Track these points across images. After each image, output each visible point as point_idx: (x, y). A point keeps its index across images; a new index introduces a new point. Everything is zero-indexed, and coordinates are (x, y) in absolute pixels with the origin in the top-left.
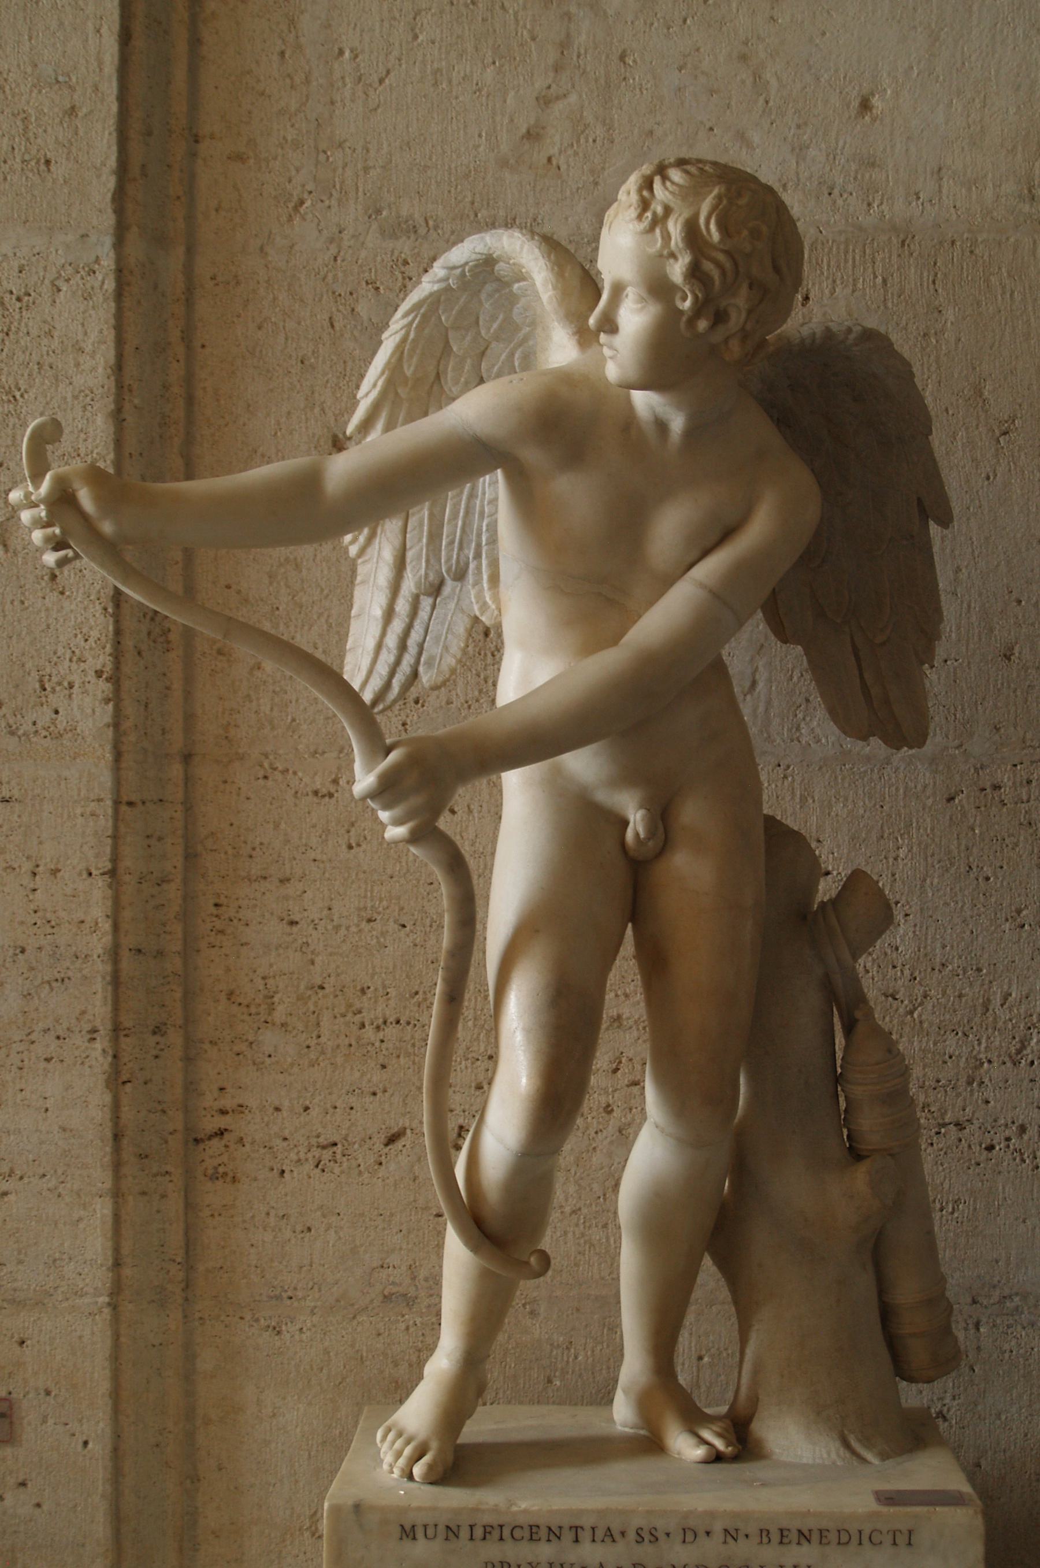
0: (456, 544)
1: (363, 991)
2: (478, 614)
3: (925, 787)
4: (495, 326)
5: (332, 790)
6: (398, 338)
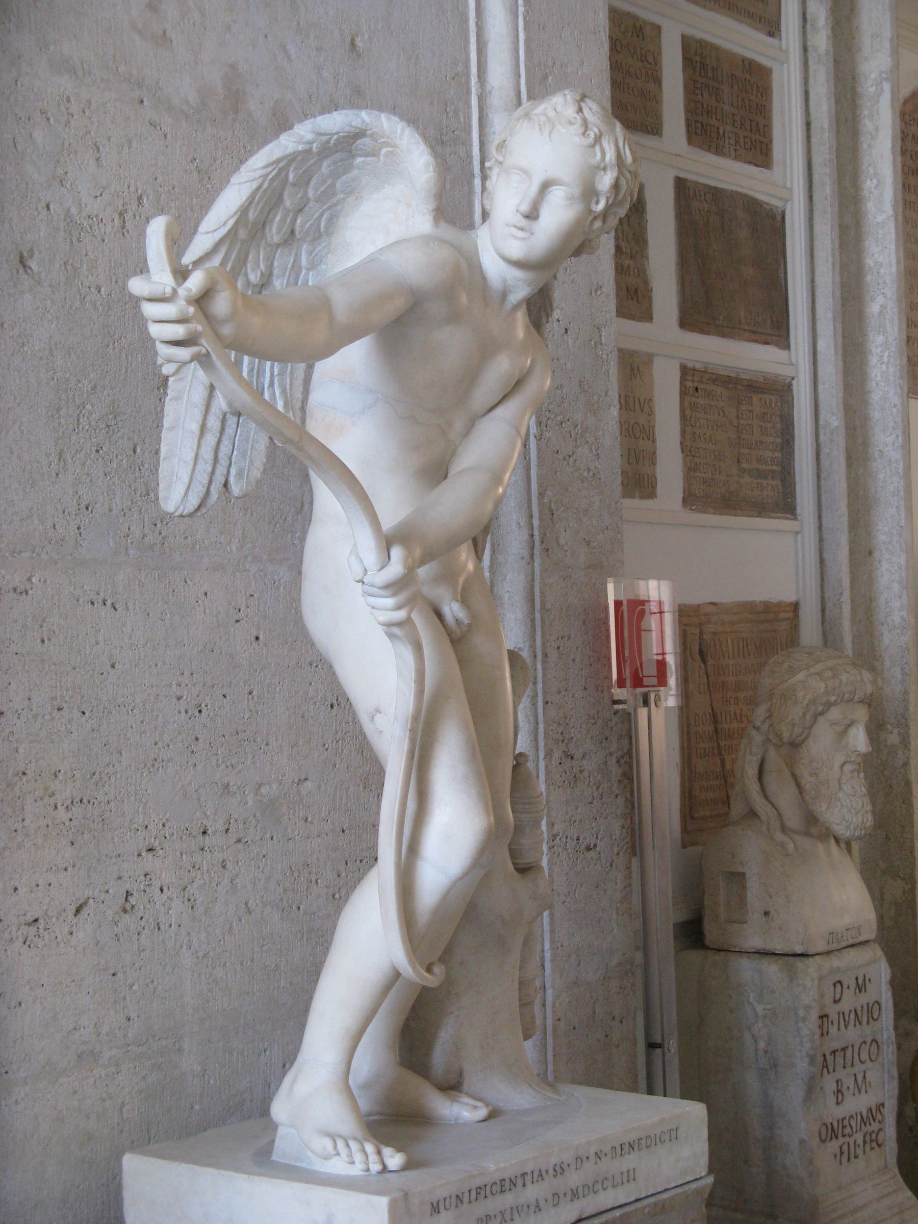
0: (255, 371)
4: (322, 189)
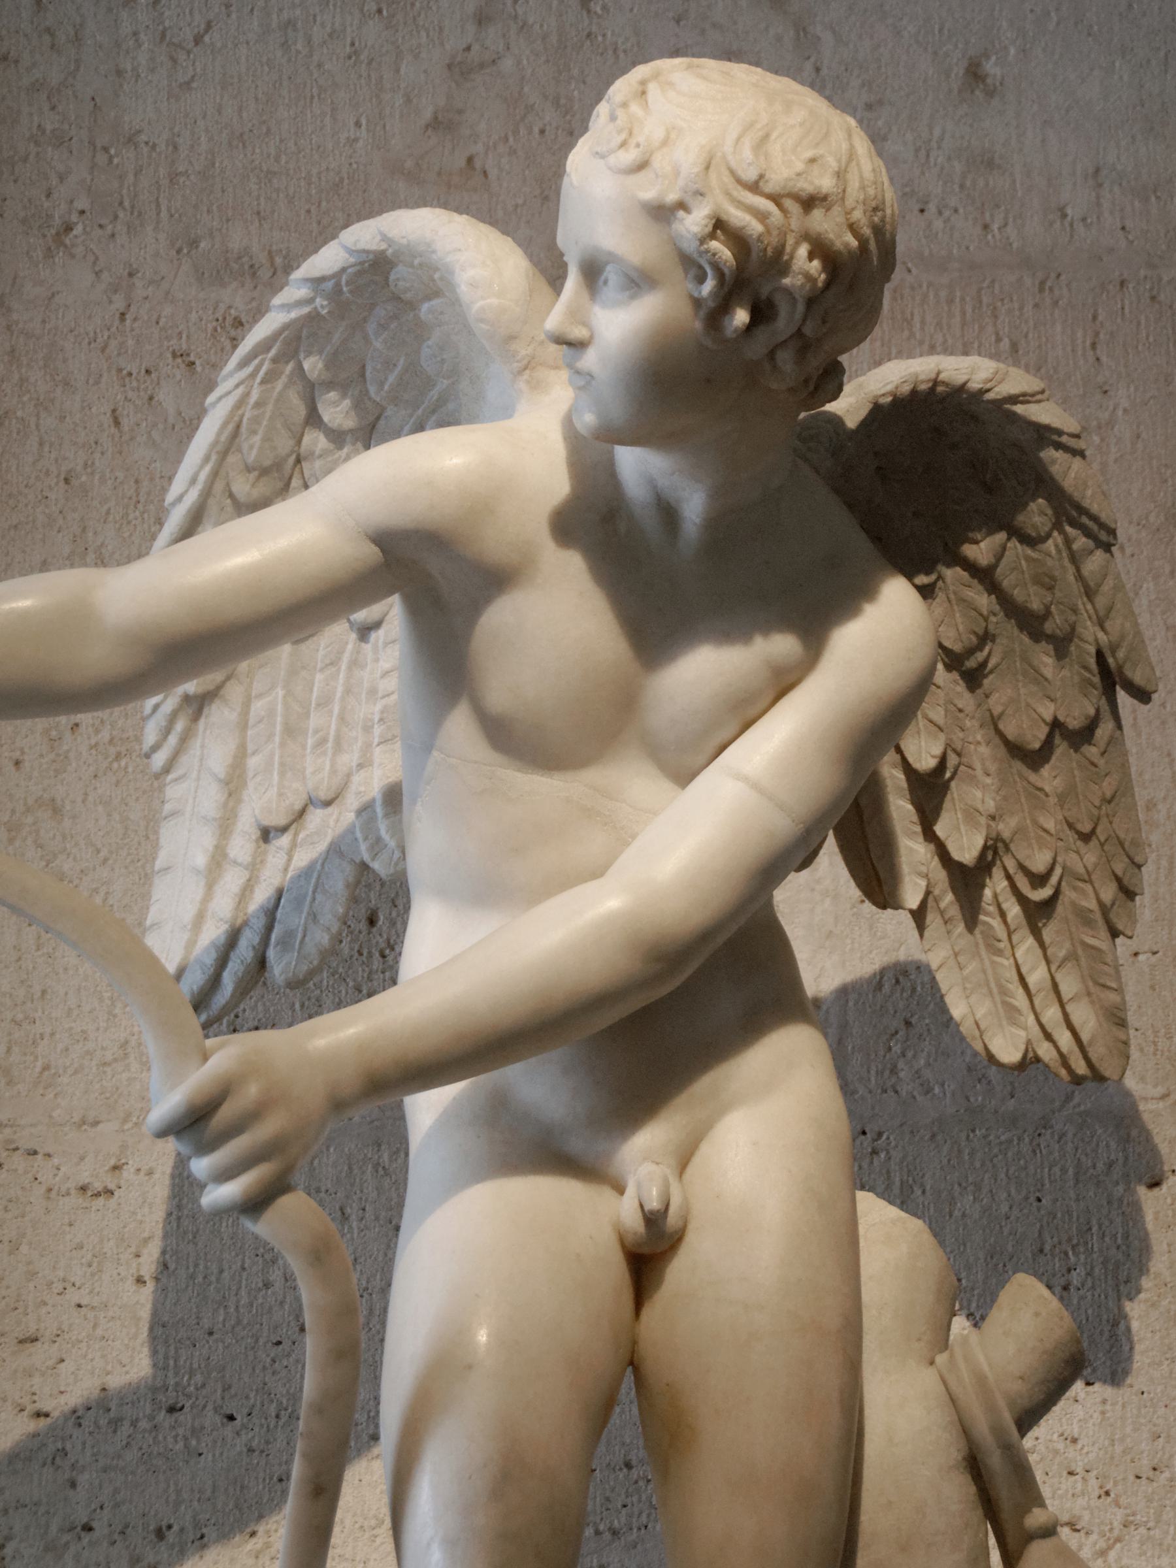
1: (160, 1534)
2: (366, 857)
3: (1110, 1165)
4: (392, 379)
5: (112, 1186)
6: (229, 402)
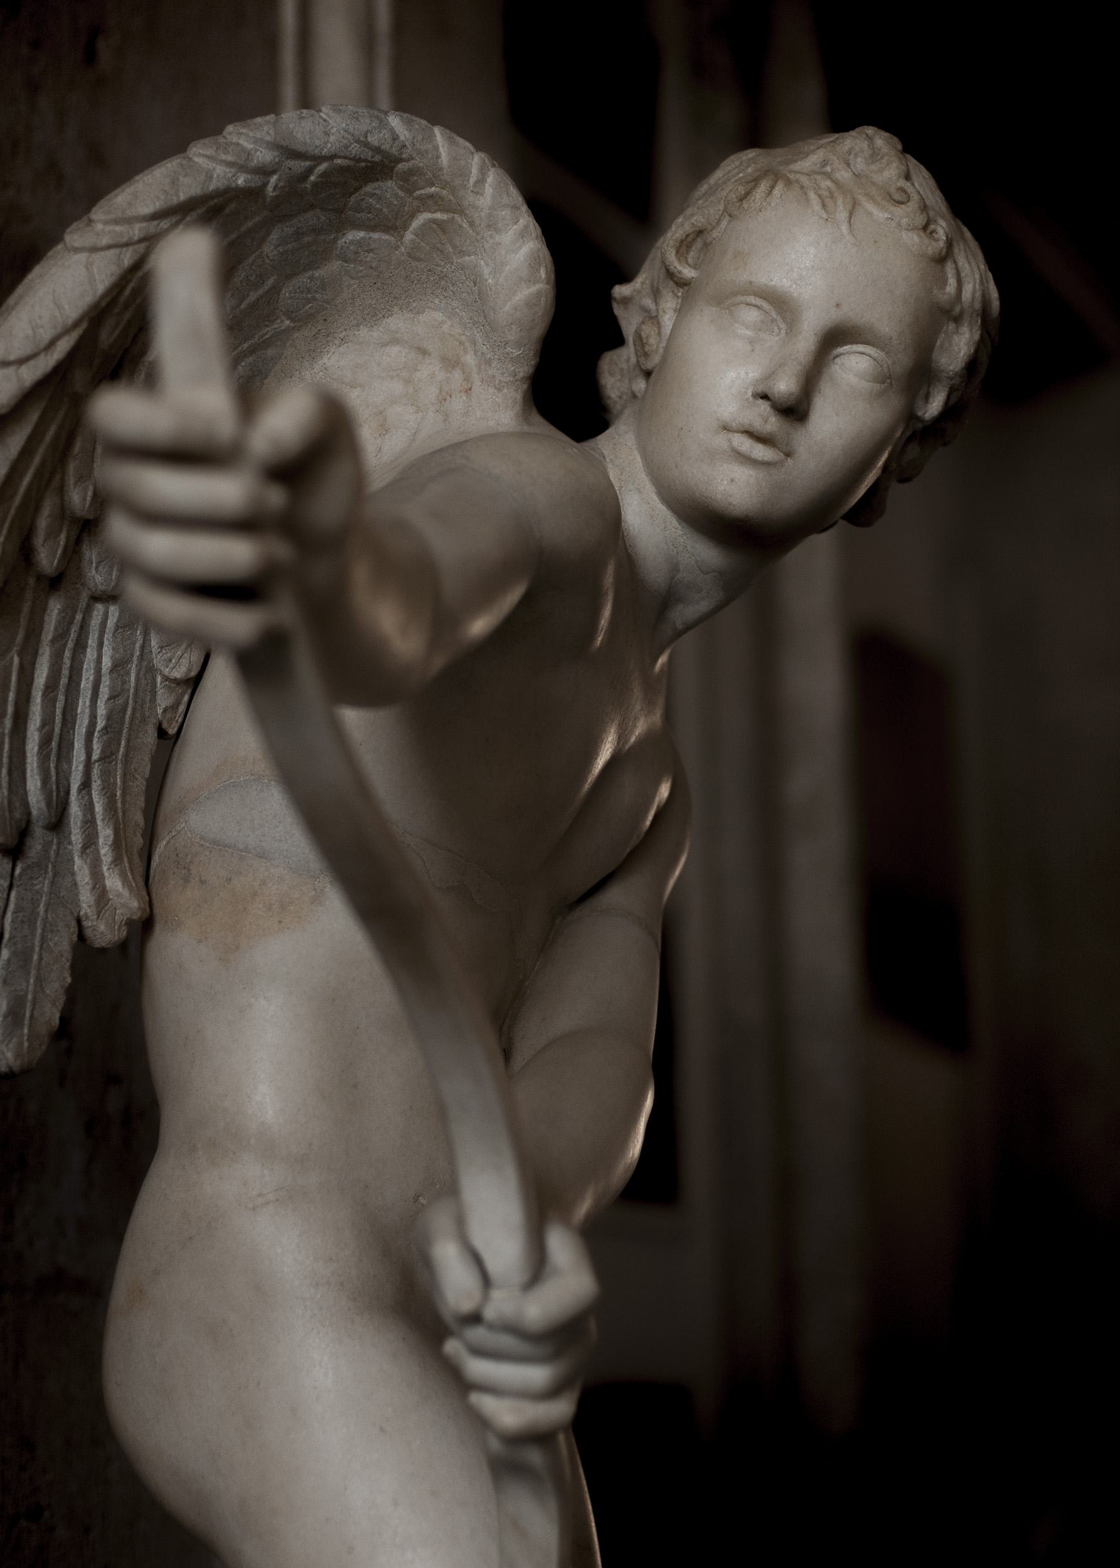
0: (54, 744)
4: (253, 296)
